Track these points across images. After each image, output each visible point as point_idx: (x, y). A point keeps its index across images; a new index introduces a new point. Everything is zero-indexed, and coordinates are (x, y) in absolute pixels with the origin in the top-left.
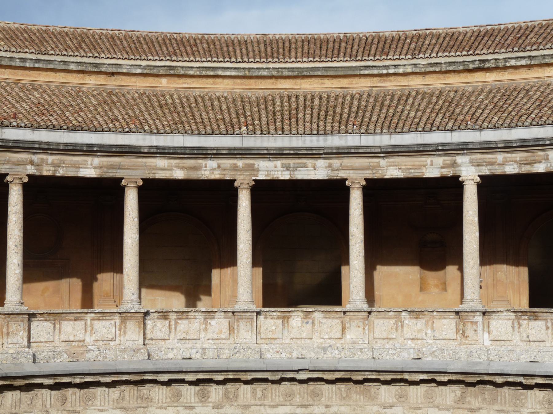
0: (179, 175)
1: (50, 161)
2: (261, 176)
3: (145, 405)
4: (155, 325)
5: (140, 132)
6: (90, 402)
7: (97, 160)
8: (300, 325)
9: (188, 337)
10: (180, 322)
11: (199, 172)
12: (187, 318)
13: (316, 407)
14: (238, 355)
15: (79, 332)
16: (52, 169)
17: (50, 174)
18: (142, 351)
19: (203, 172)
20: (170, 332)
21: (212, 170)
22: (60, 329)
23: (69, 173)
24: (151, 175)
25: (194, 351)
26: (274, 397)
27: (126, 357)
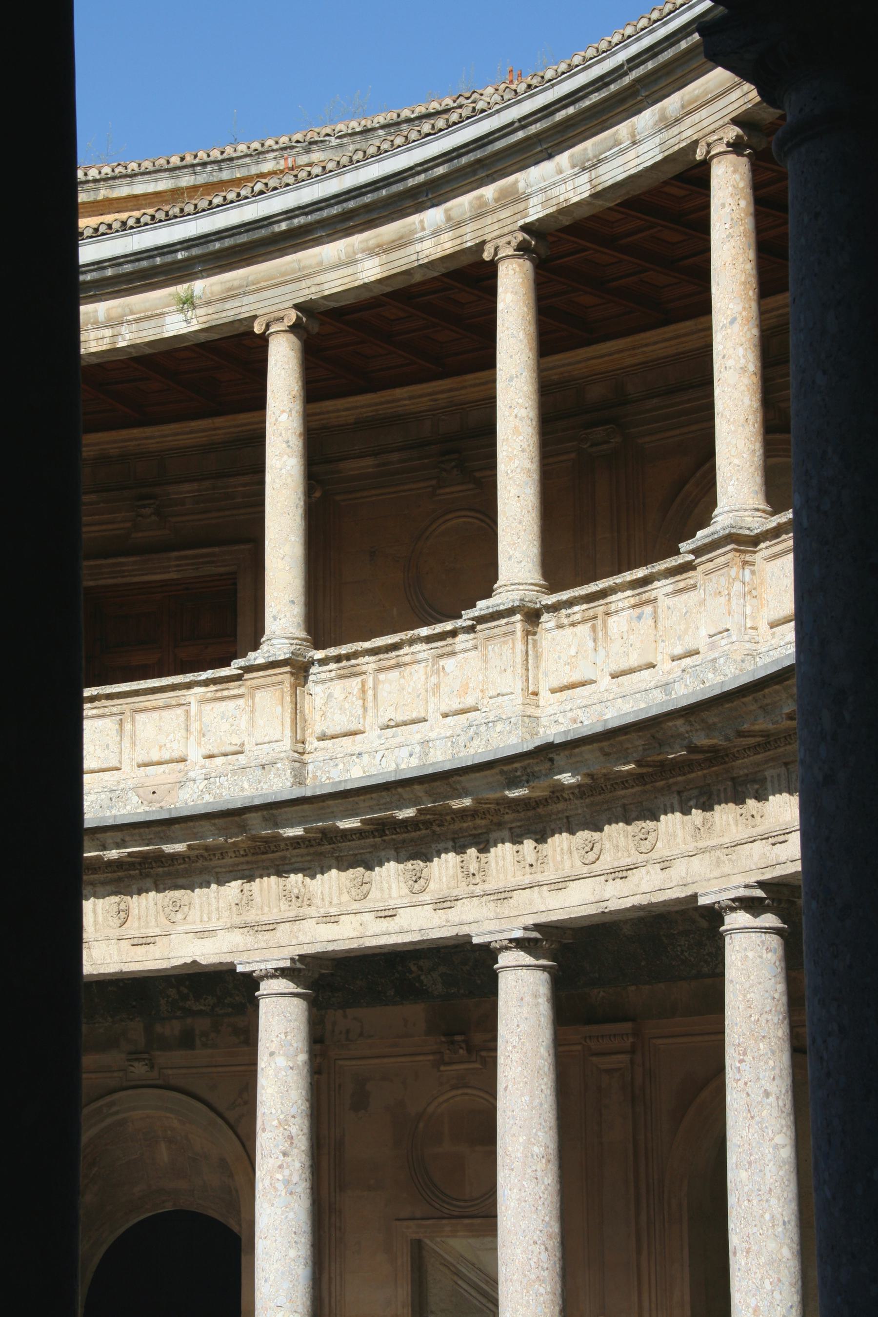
0: (371, 271)
1: (101, 317)
2: (535, 212)
3: (291, 914)
4: (330, 696)
5: (288, 185)
6: (180, 916)
7: (200, 286)
8: (625, 629)
9: (400, 718)
10: (382, 676)
11: (411, 249)
12: (398, 665)
13: (643, 870)
14: (476, 742)
15: (171, 737)
16: (108, 332)
17: (104, 348)
18: (279, 765)
19: (418, 247)
20: (365, 709)
21: (436, 233)
22: (133, 734)
23: (144, 333)
24: (313, 290)
25: (405, 752)
26: (559, 858)
27: (246, 786)
